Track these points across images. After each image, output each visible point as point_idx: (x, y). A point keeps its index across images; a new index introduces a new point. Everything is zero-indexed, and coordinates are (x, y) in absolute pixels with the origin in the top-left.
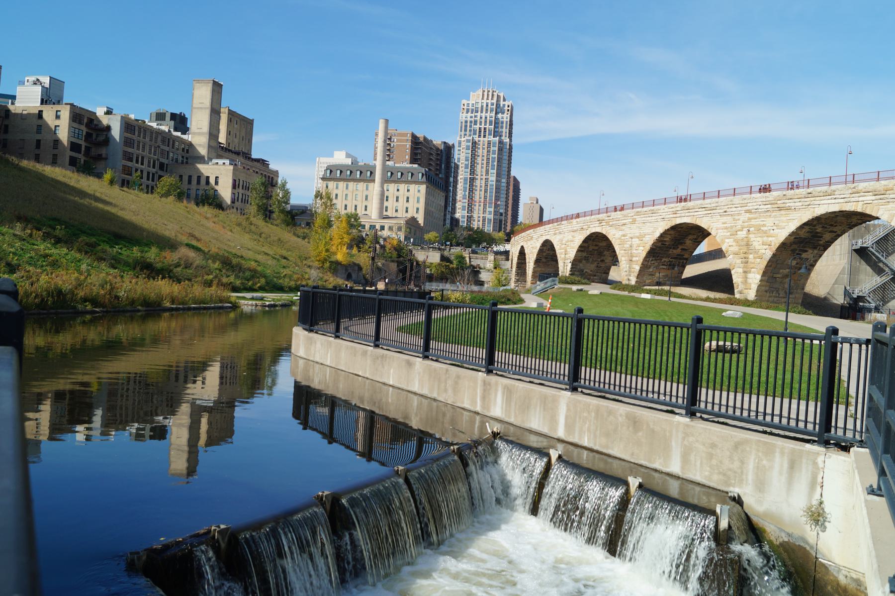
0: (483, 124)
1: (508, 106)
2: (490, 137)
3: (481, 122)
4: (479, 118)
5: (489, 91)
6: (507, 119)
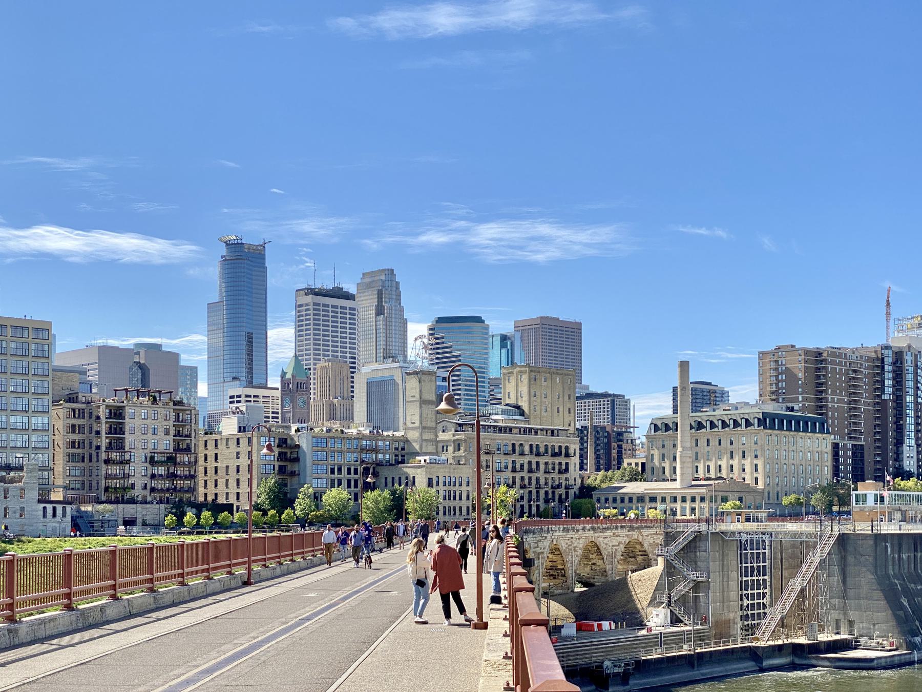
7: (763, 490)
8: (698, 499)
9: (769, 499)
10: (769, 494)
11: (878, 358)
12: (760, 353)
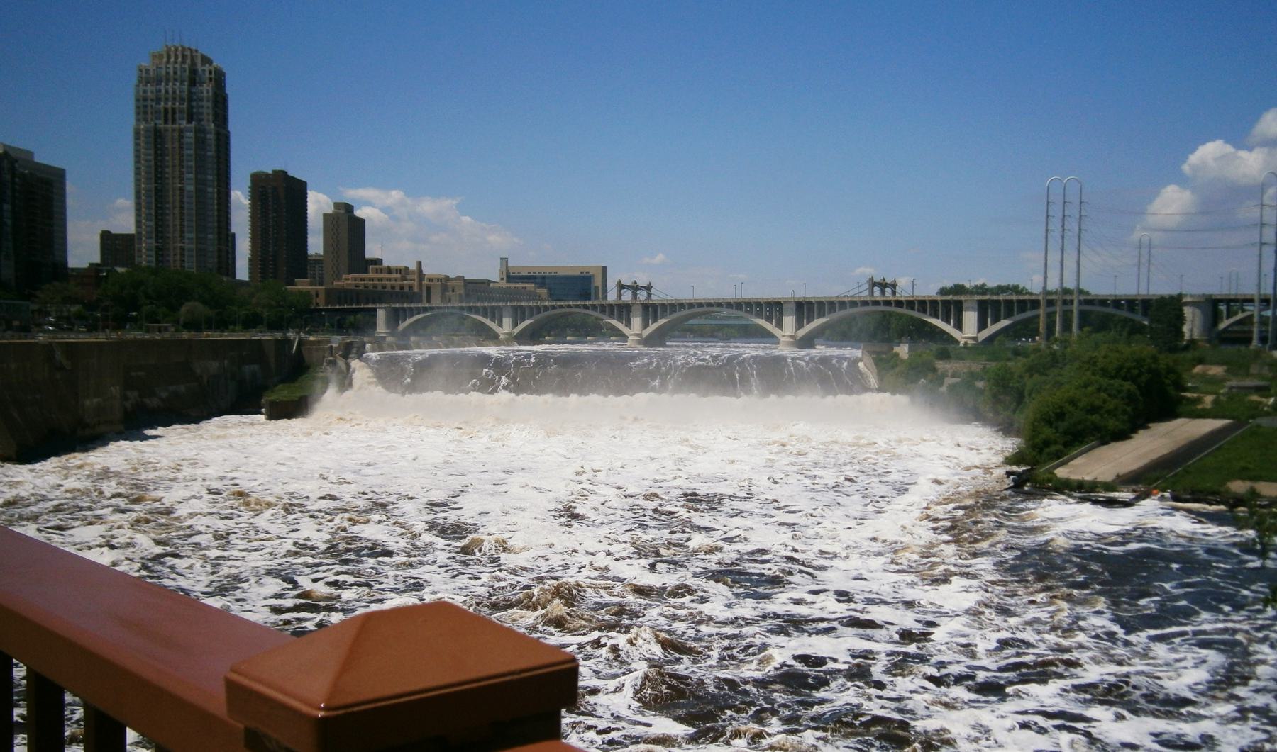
0: (170, 104)
1: (210, 73)
2: (181, 122)
4: (163, 91)
6: (208, 92)
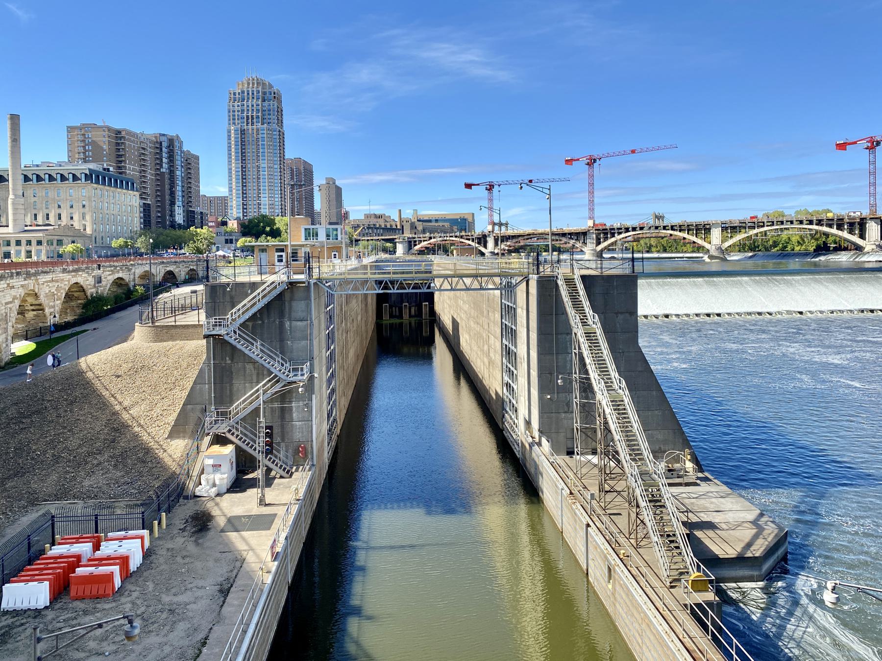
0: (250, 113)
2: (258, 124)
3: (248, 110)
4: (245, 106)
5: (253, 80)
7: (91, 235)
8: (34, 243)
9: (96, 243)
10: (95, 238)
11: (157, 142)
12: (68, 127)
